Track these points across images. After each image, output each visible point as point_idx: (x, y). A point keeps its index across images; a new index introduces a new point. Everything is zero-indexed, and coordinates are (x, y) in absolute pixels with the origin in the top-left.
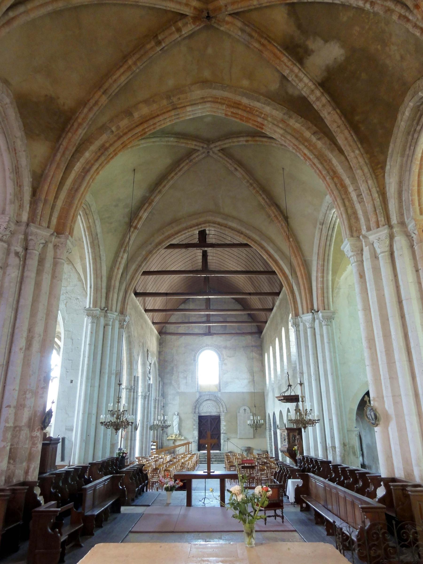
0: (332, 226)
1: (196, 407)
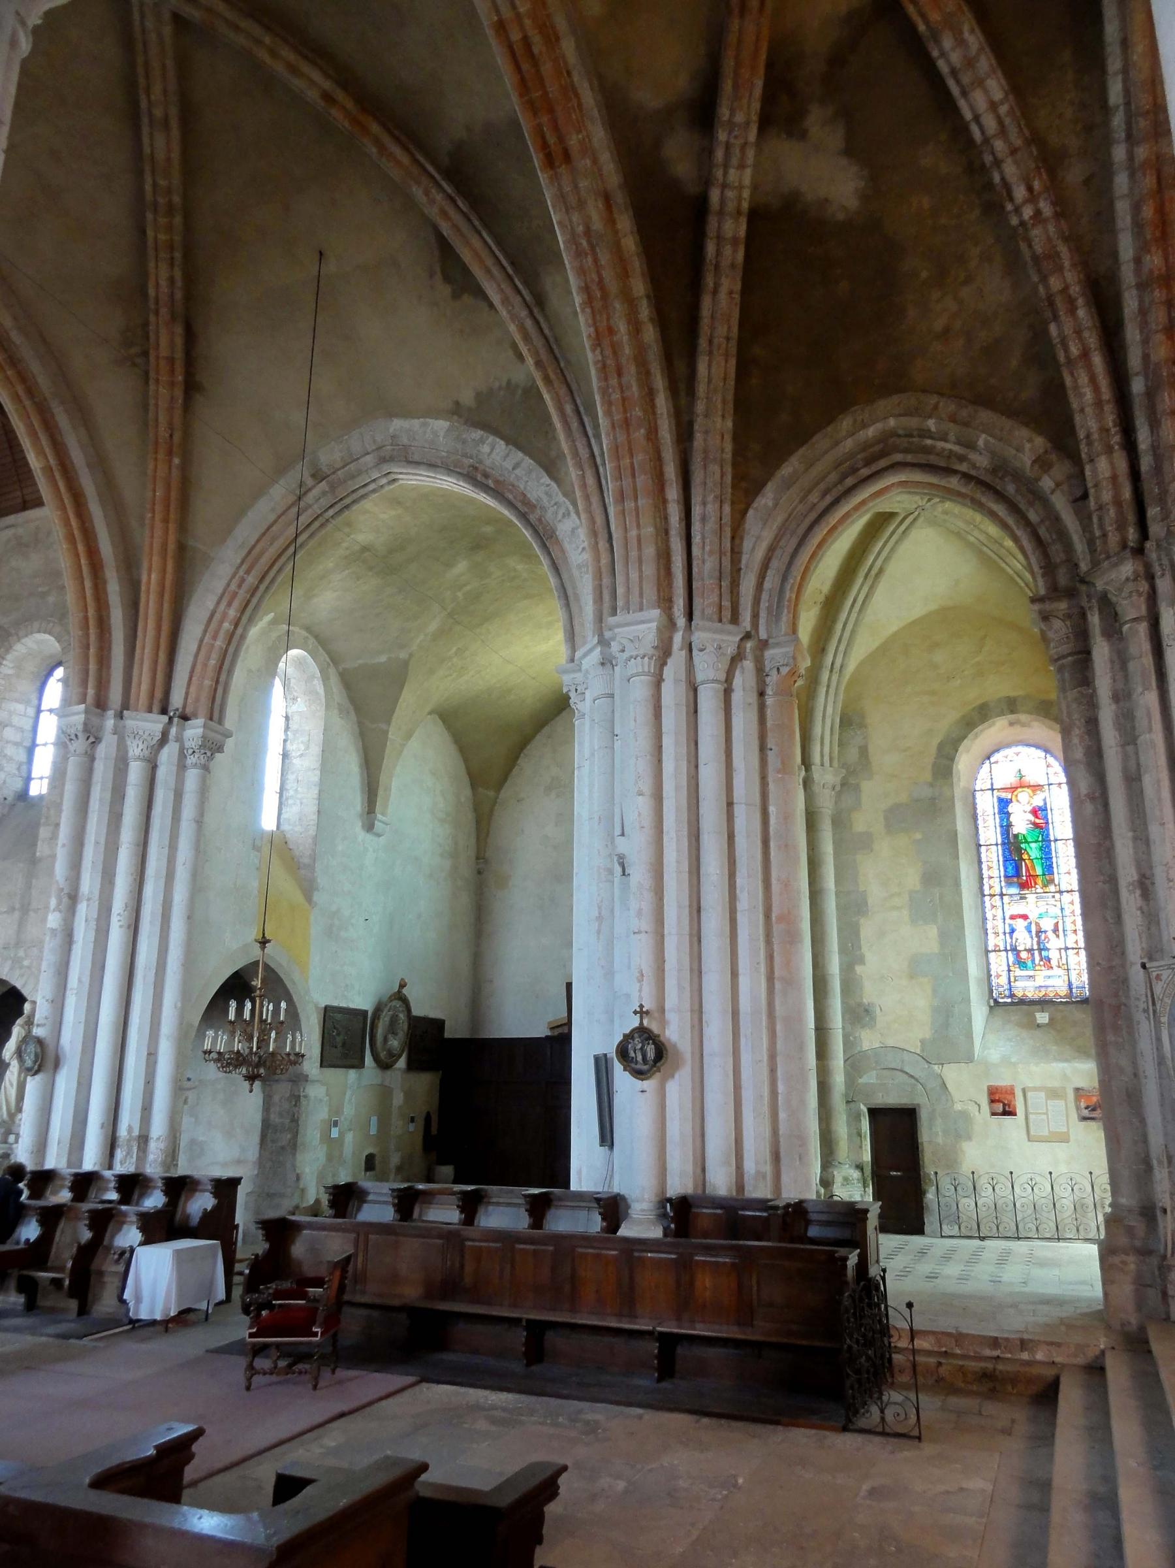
0: (347, 501)
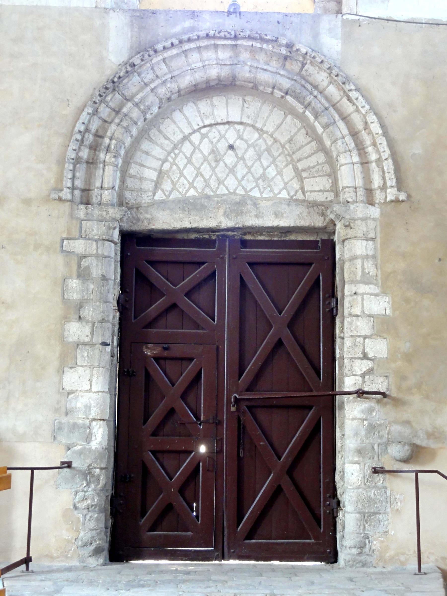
1: (94, 148)
